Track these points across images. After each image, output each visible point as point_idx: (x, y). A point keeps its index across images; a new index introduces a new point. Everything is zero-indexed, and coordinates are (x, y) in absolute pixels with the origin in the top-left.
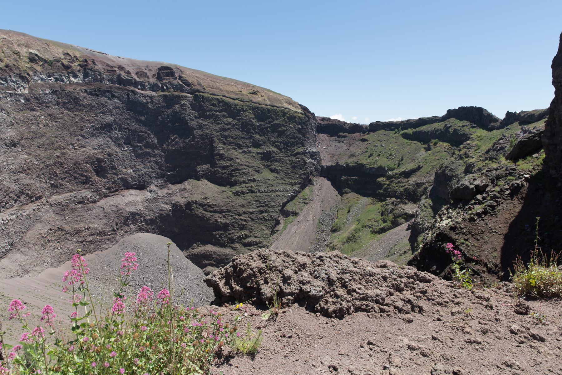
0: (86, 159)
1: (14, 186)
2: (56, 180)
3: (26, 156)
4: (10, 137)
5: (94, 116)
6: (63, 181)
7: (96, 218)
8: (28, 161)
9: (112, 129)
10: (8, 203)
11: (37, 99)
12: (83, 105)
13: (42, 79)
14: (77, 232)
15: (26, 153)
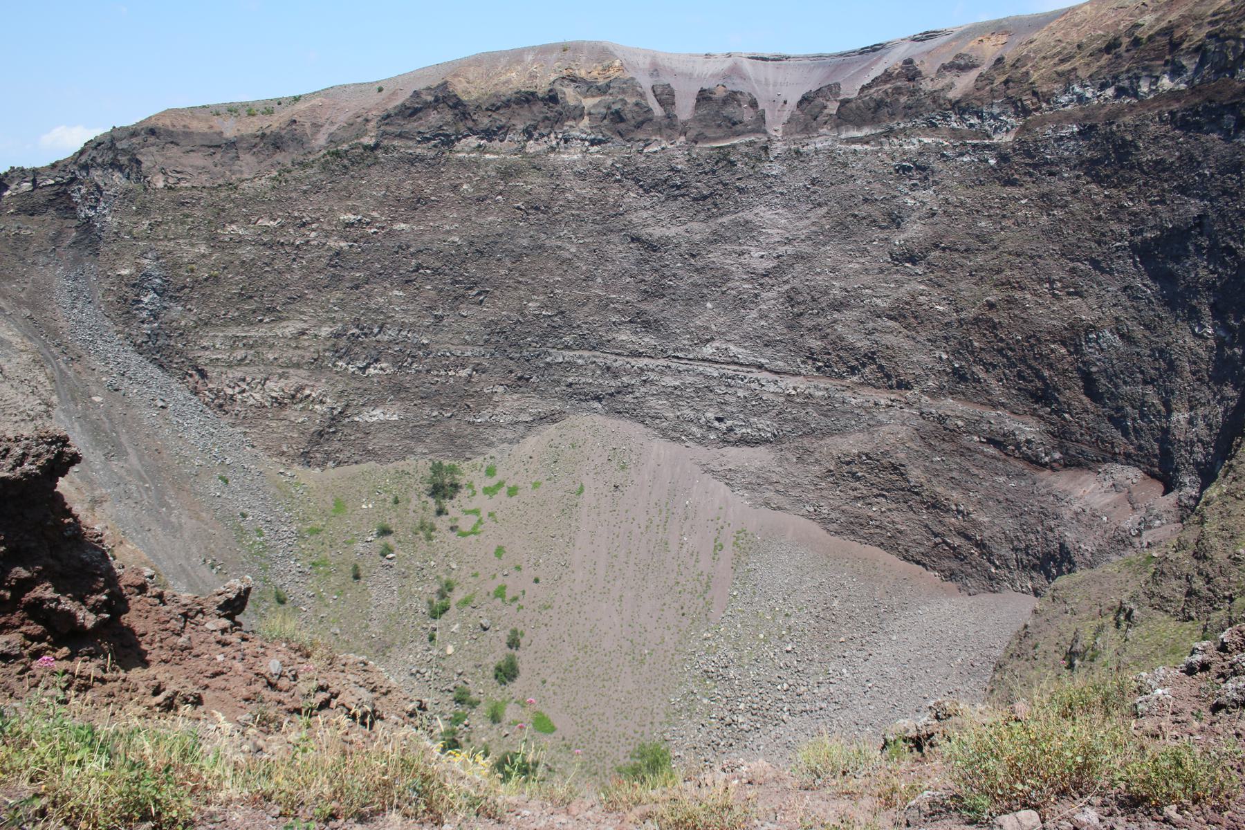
0: (1065, 332)
1: (860, 340)
2: (967, 361)
3: (922, 287)
4: (906, 241)
5: (1157, 202)
6: (987, 371)
7: (1004, 504)
8: (922, 299)
9: (1186, 249)
10: (830, 366)
11: (1028, 154)
12: (1140, 164)
13: (1081, 99)
14: (935, 505)
15: (930, 280)
